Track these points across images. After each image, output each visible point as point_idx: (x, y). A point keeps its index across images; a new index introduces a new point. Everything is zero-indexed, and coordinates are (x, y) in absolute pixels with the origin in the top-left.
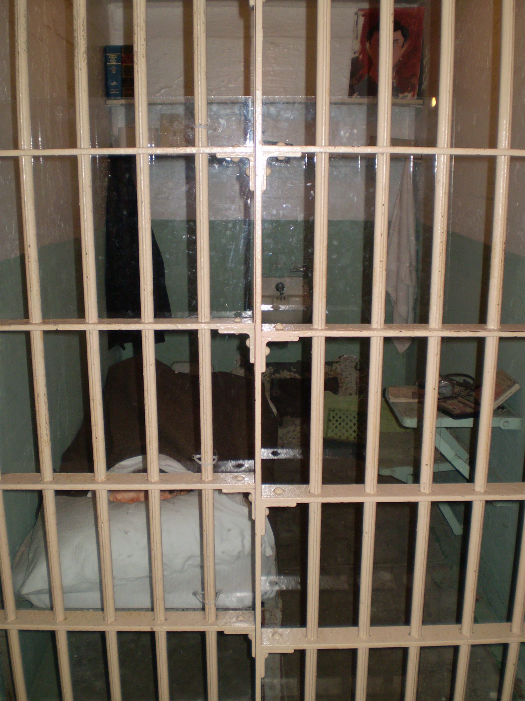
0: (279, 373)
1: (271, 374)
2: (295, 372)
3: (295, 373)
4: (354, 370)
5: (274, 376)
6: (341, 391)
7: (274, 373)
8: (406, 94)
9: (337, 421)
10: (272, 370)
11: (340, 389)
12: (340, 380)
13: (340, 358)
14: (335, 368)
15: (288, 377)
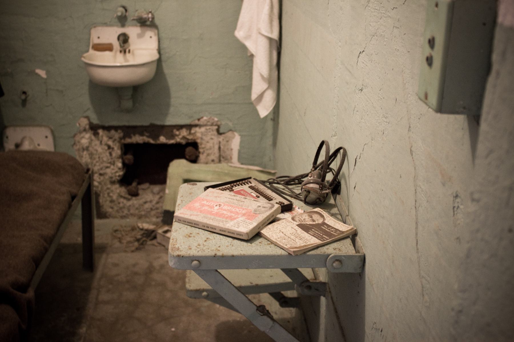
1: (121, 139)
2: (148, 137)
6: (202, 157)
7: (124, 137)
10: (122, 135)
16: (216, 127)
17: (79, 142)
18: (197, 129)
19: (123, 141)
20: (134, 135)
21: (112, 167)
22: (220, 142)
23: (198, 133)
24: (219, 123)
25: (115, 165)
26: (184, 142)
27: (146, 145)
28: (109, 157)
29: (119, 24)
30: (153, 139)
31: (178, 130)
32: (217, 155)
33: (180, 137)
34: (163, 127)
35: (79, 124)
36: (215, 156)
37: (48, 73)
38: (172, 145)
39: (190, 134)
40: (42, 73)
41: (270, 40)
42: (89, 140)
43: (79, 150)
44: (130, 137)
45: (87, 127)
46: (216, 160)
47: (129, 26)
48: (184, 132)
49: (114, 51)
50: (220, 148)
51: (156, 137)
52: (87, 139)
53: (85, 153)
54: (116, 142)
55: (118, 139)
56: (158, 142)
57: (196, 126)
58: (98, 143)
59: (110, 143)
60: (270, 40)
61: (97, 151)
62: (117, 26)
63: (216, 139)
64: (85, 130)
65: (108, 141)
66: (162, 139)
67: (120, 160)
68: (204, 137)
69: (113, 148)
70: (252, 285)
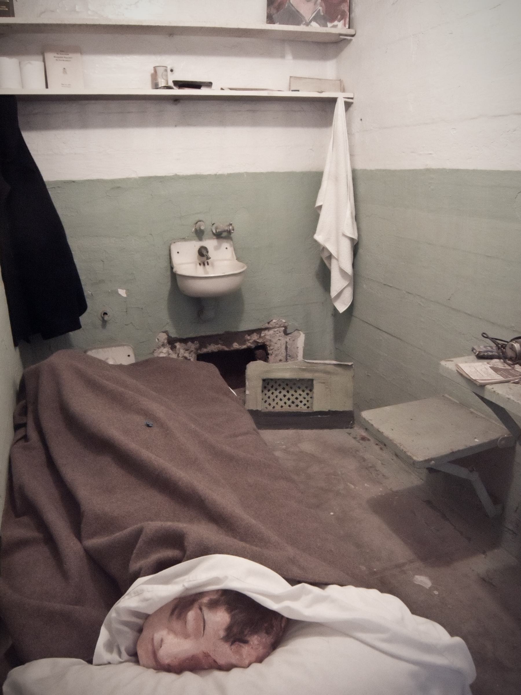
1: (197, 349)
2: (223, 345)
3: (223, 345)
8: (336, 23)
9: (297, 398)
10: (198, 345)
11: (270, 357)
12: (270, 347)
14: (264, 335)
15: (216, 350)
16: (283, 328)
18: (266, 332)
19: (199, 351)
22: (286, 343)
24: (286, 324)
26: (253, 346)
29: (196, 238)
30: (227, 347)
31: (249, 335)
32: (284, 354)
33: (251, 341)
35: (158, 339)
36: (282, 356)
37: (128, 291)
39: (260, 337)
40: (122, 292)
41: (352, 240)
44: (206, 347)
45: (166, 341)
46: (284, 359)
47: (206, 239)
48: (255, 337)
50: (286, 348)
51: (230, 344)
54: (192, 353)
55: (195, 350)
56: (232, 348)
59: (187, 355)
60: (352, 240)
63: (284, 339)
64: (163, 345)
66: (236, 346)
68: (273, 340)
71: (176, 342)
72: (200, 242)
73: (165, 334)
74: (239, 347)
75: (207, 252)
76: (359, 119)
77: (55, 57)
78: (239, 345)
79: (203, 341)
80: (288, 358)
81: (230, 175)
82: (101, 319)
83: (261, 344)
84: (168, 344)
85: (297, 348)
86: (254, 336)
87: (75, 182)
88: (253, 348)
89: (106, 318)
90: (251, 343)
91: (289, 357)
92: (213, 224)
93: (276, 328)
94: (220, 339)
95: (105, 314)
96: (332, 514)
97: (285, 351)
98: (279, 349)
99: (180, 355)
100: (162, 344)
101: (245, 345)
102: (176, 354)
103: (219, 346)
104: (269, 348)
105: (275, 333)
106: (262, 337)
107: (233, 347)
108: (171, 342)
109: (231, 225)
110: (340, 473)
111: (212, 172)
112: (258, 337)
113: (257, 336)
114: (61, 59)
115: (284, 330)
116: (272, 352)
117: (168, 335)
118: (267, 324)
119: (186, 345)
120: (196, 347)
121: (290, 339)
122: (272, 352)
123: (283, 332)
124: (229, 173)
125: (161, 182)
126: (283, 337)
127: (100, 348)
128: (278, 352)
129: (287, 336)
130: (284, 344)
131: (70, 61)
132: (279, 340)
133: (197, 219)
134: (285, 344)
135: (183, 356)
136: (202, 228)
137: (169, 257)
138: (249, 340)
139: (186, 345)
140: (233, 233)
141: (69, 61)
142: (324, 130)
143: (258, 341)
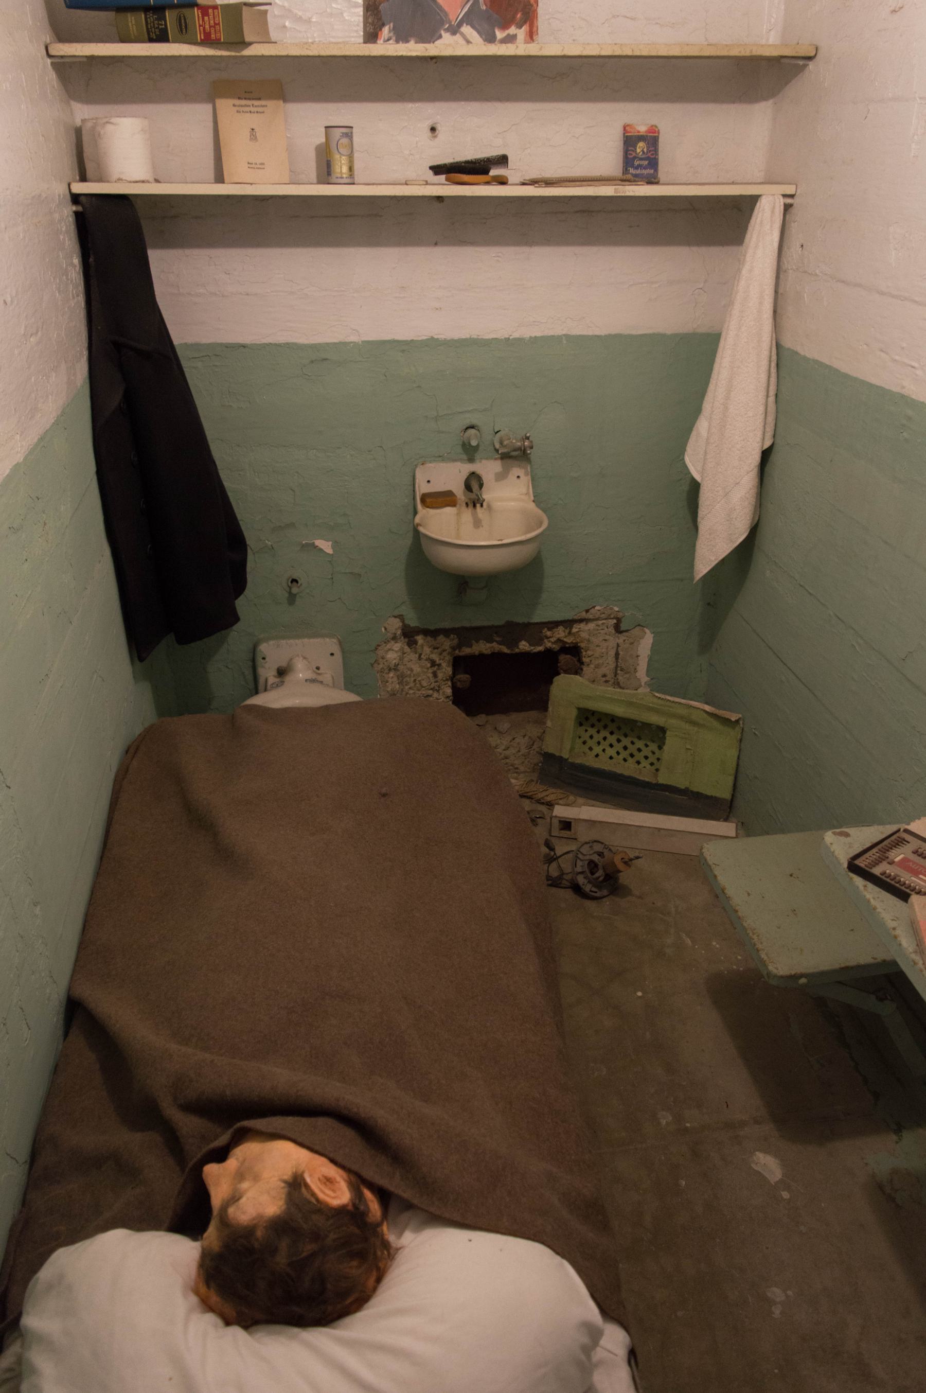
0: (471, 646)
1: (453, 648)
2: (499, 643)
3: (500, 644)
4: (613, 631)
5: (459, 651)
10: (456, 641)
11: (585, 668)
12: (586, 651)
13: (587, 611)
14: (577, 630)
15: (488, 652)
16: (615, 621)
17: (383, 658)
18: (582, 625)
20: (477, 642)
21: (435, 695)
22: (618, 645)
23: (583, 631)
24: (619, 615)
25: (441, 692)
26: (556, 647)
27: (498, 655)
28: (432, 680)
30: (508, 648)
31: (549, 629)
32: (612, 666)
33: (553, 640)
34: (528, 625)
35: (386, 629)
37: (336, 544)
38: (540, 652)
39: (570, 633)
40: (326, 546)
42: (399, 654)
43: (382, 671)
45: (399, 632)
48: (560, 633)
49: (458, 506)
50: (617, 655)
51: (516, 643)
52: (396, 652)
53: (391, 675)
55: (449, 650)
56: (517, 650)
57: (581, 621)
58: (414, 657)
59: (435, 657)
61: (412, 670)
62: (461, 460)
63: (613, 641)
64: (394, 638)
65: (432, 653)
67: (450, 683)
68: (593, 639)
69: (439, 665)
70: (876, 961)
71: (418, 635)
72: (471, 464)
73: (398, 620)
74: (529, 649)
75: (481, 486)
76: (798, 245)
77: (234, 105)
78: (530, 645)
79: (466, 634)
80: (619, 672)
81: (534, 340)
82: (288, 589)
83: (571, 645)
84: (403, 637)
85: (638, 656)
86: (559, 631)
87: (247, 347)
88: (556, 650)
89: (295, 590)
90: (553, 643)
91: (621, 670)
92: (496, 431)
93: (600, 620)
94: (496, 633)
95: (294, 581)
96: (639, 994)
97: (614, 659)
98: (603, 656)
99: (422, 656)
100: (392, 636)
101: (541, 646)
102: (416, 653)
103: (494, 644)
104: (584, 653)
105: (597, 627)
106: (574, 633)
107: (518, 648)
108: (409, 634)
109: (528, 438)
110: (673, 910)
111: (502, 334)
112: (567, 634)
113: (564, 632)
114: (248, 109)
115: (615, 623)
116: (591, 661)
117: (403, 622)
118: (584, 613)
119: (435, 639)
120: (451, 645)
121: (624, 641)
122: (591, 661)
123: (614, 627)
124: (533, 335)
125: (403, 351)
126: (612, 637)
127: (283, 638)
128: (601, 661)
129: (619, 635)
130: (613, 648)
131: (263, 112)
132: (605, 640)
133: (468, 422)
134: (615, 649)
135: (429, 658)
136: (474, 443)
137: (412, 479)
138: (550, 637)
139: (435, 639)
140: (530, 454)
141: (260, 113)
142: (732, 249)
143: (565, 640)
